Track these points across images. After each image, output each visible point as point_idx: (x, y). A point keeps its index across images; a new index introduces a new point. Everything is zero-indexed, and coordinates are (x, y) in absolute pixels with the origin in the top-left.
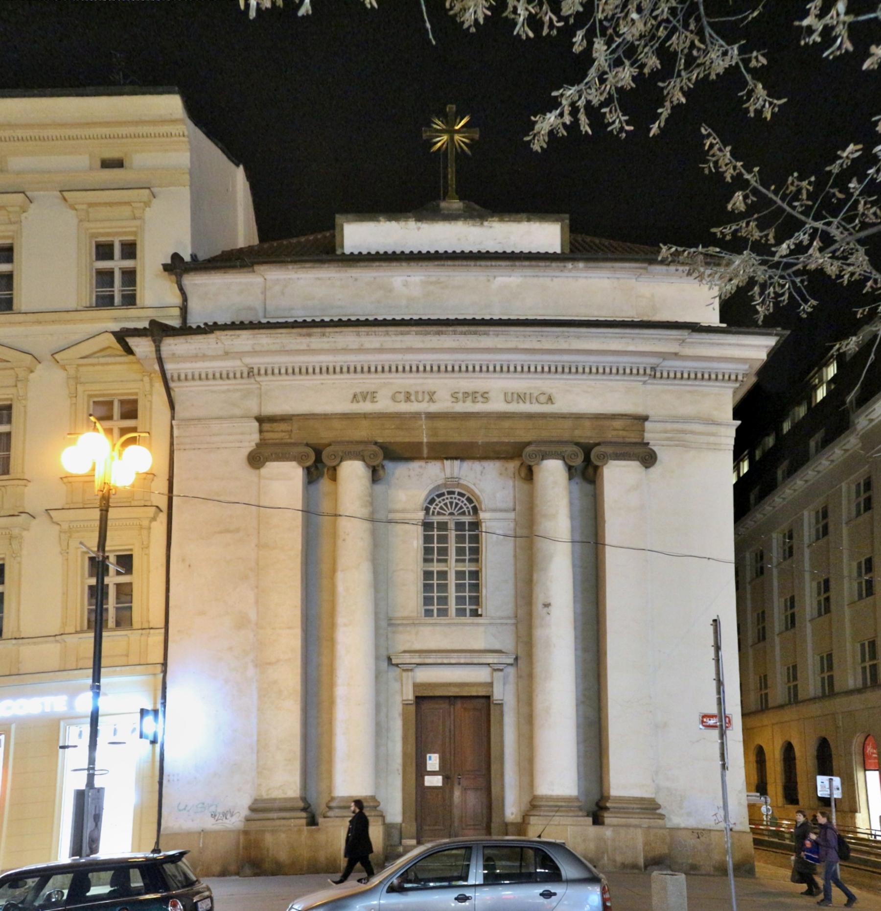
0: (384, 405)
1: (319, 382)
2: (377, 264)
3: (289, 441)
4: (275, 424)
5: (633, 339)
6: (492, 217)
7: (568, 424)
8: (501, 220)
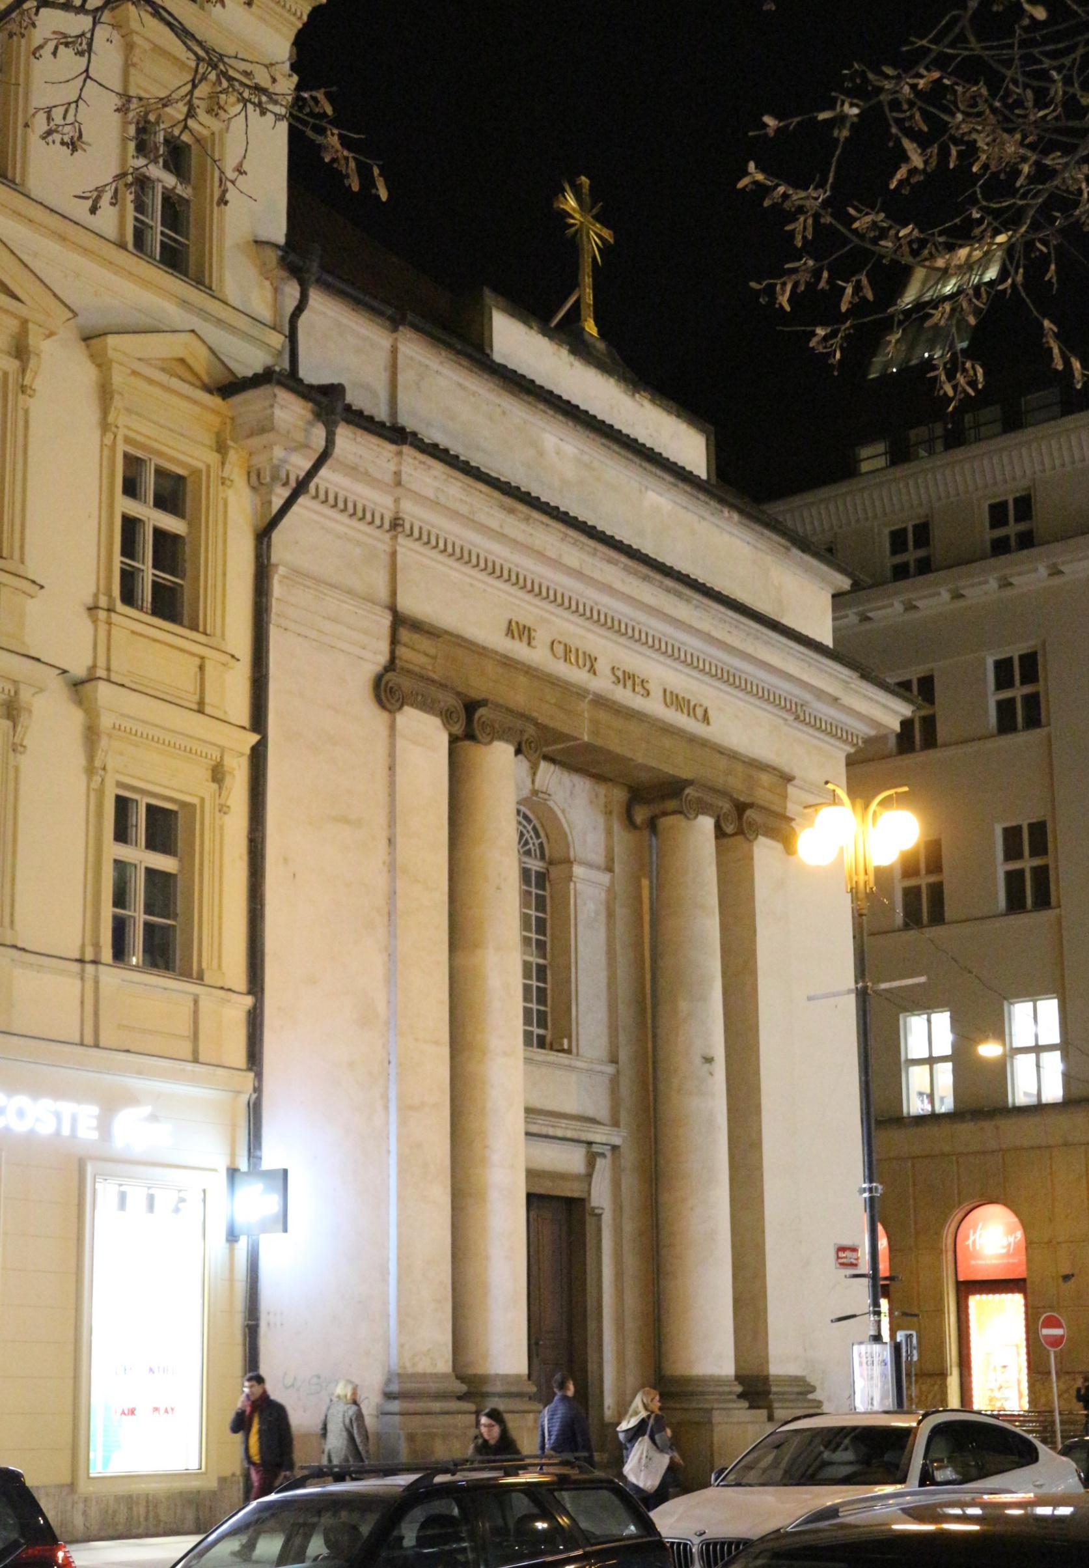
0: (537, 655)
1: (468, 580)
2: (530, 399)
3: (431, 675)
4: (416, 636)
5: (810, 665)
6: (645, 391)
7: (723, 763)
8: (652, 401)
